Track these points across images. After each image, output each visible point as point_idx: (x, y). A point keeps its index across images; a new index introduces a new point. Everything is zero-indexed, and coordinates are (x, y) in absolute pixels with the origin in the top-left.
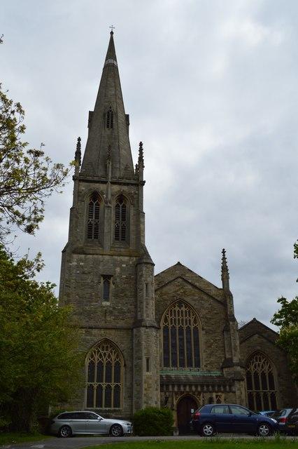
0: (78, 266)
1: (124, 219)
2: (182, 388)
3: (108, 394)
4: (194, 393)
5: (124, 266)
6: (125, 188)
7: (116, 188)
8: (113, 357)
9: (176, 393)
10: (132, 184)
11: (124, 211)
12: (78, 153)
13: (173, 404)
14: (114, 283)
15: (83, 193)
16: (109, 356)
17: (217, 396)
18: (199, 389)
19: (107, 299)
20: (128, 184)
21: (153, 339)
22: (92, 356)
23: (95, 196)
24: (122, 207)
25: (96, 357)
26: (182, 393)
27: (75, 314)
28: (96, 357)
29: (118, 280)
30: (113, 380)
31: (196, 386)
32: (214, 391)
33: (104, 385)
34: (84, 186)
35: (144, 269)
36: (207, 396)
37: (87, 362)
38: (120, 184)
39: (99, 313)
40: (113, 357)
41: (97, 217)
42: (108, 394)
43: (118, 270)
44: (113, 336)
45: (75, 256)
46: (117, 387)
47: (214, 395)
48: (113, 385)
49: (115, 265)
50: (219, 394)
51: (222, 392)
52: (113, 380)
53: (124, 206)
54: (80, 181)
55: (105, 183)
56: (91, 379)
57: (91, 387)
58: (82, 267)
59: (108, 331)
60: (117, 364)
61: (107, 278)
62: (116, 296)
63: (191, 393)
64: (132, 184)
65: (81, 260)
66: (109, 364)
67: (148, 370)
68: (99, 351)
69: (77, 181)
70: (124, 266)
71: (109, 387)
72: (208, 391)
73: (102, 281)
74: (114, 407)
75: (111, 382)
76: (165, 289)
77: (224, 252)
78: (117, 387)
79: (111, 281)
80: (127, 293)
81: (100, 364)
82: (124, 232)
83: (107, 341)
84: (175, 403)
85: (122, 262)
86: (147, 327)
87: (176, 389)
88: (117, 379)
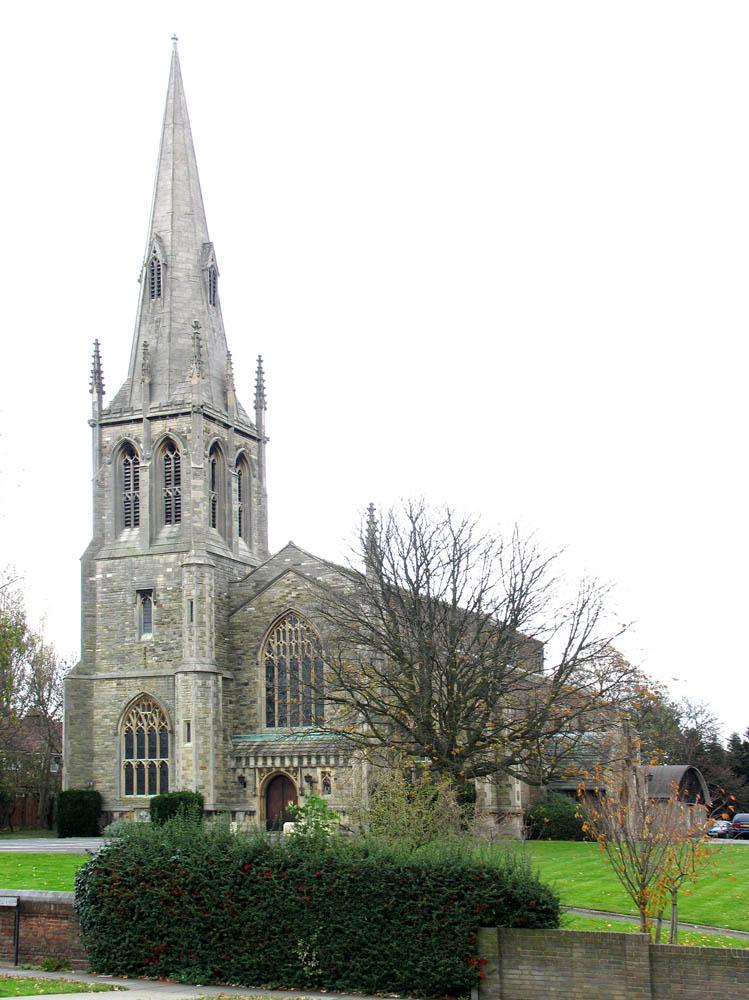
0: (106, 581)
1: (178, 481)
2: (269, 762)
3: (152, 774)
4: (287, 769)
5: (169, 570)
6: (172, 423)
7: (158, 427)
8: (156, 720)
9: (260, 770)
10: (183, 414)
11: (177, 466)
12: (97, 373)
13: (255, 788)
14: (155, 603)
15: (108, 448)
16: (152, 719)
17: (324, 773)
18: (296, 763)
19: (146, 626)
20: (175, 416)
21: (193, 691)
22: (129, 720)
23: (128, 448)
24: (175, 459)
25: (134, 721)
26: (269, 769)
27: (103, 659)
28: (134, 721)
29: (161, 596)
30: (158, 755)
31: (291, 758)
32: (318, 764)
33: (146, 762)
34: (111, 436)
35: (186, 575)
36: (305, 772)
37: (122, 732)
38: (163, 417)
39: (136, 653)
40: (156, 720)
41: (136, 487)
42: (152, 774)
43: (160, 579)
44: (151, 688)
45: (99, 564)
46: (163, 764)
47: (319, 770)
48: (157, 761)
49: (156, 572)
50: (328, 770)
51: (332, 767)
52: (158, 755)
53: (177, 457)
54: (102, 425)
55: (139, 421)
56: (129, 754)
57: (129, 766)
58: (109, 580)
59: (147, 681)
60: (163, 729)
61: (145, 594)
62: (160, 623)
63: (282, 770)
64: (183, 414)
65: (109, 571)
66: (151, 730)
67: (189, 740)
68: (137, 713)
69: (97, 427)
70: (169, 570)
71: (152, 765)
72: (309, 766)
73: (139, 597)
74: (138, 793)
75: (155, 757)
76: (267, 594)
77: (371, 510)
78: (163, 764)
79: (152, 599)
80: (174, 616)
81: (140, 731)
82: (178, 508)
83: (145, 696)
84: (258, 786)
85: (167, 565)
86: (186, 673)
87: (260, 763)
88: (164, 754)
